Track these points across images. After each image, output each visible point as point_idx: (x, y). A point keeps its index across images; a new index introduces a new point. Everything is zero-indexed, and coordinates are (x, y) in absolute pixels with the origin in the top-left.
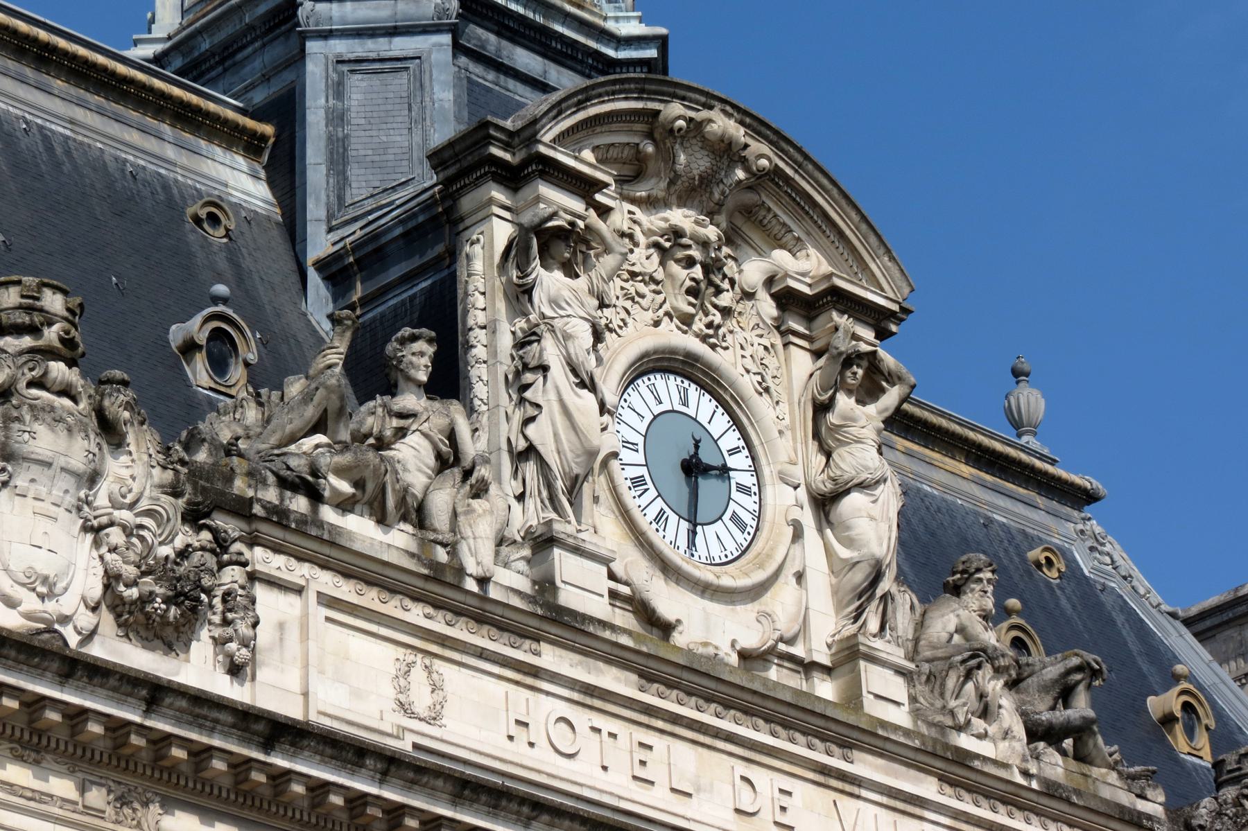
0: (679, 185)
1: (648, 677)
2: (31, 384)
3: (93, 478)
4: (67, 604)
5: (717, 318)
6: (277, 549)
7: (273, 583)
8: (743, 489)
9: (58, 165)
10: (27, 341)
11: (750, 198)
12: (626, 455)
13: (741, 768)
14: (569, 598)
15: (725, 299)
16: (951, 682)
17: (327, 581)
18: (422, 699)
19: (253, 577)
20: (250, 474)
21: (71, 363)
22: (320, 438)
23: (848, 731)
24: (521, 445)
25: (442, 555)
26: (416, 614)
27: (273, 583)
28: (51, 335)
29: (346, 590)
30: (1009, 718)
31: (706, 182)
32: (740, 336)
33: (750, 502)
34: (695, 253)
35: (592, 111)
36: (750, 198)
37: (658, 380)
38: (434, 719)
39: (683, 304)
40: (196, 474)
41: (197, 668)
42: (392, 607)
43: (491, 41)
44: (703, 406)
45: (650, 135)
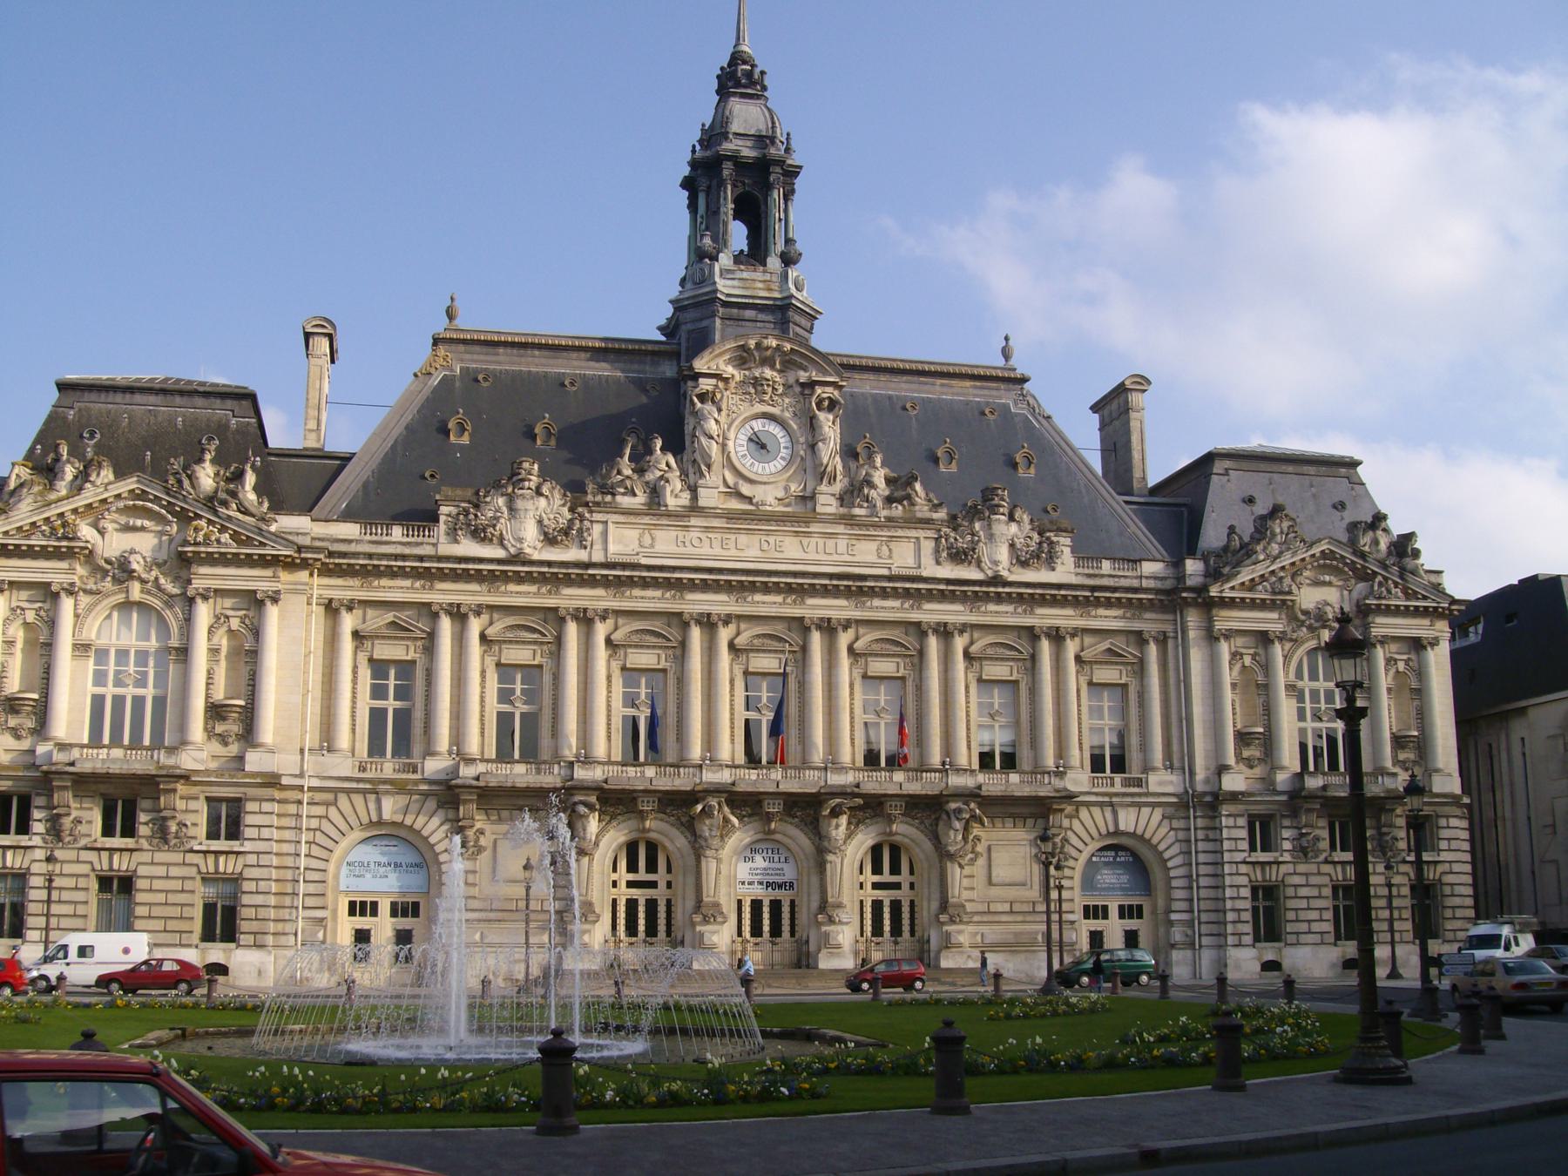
14: (701, 503)
23: (811, 516)
26: (647, 520)
29: (621, 518)
38: (652, 546)
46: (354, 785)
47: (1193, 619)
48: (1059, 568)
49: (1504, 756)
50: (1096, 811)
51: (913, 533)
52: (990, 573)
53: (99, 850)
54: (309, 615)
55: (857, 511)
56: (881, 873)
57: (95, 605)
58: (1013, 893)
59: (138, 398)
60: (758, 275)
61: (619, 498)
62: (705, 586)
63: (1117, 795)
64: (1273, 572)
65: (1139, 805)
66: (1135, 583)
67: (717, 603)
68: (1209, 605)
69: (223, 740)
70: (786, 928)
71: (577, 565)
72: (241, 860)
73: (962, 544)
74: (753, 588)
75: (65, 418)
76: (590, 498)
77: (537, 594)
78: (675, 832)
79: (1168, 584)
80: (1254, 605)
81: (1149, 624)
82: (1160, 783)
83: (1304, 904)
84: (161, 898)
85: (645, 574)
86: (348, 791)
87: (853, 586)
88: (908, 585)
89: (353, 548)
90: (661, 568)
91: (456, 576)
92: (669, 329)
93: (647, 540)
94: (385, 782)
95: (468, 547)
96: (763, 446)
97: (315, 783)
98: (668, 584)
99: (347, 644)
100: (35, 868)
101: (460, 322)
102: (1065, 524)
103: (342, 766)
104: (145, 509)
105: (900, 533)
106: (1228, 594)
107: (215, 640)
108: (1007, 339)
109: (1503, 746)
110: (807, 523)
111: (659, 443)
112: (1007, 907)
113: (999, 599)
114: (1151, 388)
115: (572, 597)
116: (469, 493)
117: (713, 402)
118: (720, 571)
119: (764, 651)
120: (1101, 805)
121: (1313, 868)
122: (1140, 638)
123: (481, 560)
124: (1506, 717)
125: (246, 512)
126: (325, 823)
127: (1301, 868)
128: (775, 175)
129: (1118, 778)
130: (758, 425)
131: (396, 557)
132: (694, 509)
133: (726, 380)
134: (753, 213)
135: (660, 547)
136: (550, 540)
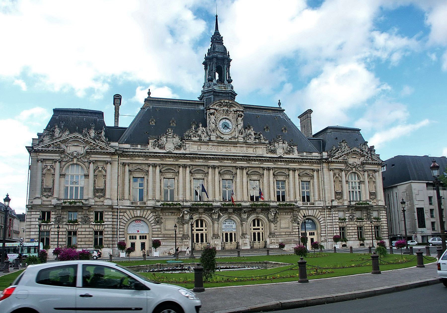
1: (218, 143)
17: (192, 143)
26: (199, 143)
29: (193, 143)
44: (227, 121)
47: (325, 165)
48: (295, 154)
49: (392, 196)
51: (261, 146)
52: (279, 156)
53: (68, 225)
54: (118, 166)
55: (248, 141)
56: (255, 226)
57: (65, 164)
58: (285, 230)
59: (74, 113)
60: (222, 85)
62: (213, 159)
63: (309, 207)
64: (343, 155)
65: (314, 209)
66: (312, 158)
67: (216, 163)
68: (329, 162)
69: (99, 197)
70: (233, 239)
71: (183, 154)
72: (104, 226)
73: (272, 148)
74: (224, 159)
75: (56, 118)
76: (185, 138)
79: (319, 158)
80: (339, 163)
81: (315, 167)
82: (318, 204)
83: (351, 231)
84: (84, 236)
86: (129, 209)
87: (247, 159)
89: (128, 150)
90: (203, 155)
91: (155, 157)
92: (201, 98)
93: (199, 148)
94: (138, 207)
95: (157, 150)
96: (226, 126)
97: (121, 207)
98: (205, 158)
99: (127, 173)
100: (52, 230)
101: (151, 96)
102: (295, 143)
103: (128, 203)
104: (78, 141)
106: (333, 160)
107: (96, 173)
109: (392, 195)
111: (201, 125)
112: (284, 234)
113: (281, 161)
115: (182, 162)
116: (156, 137)
117: (214, 115)
118: (217, 155)
120: (305, 209)
121: (353, 223)
122: (313, 170)
123: (160, 153)
124: (392, 188)
125: (103, 142)
127: (351, 223)
128: (226, 62)
129: (309, 203)
130: (224, 121)
131: (139, 152)
132: (210, 140)
133: (217, 110)
134: (220, 70)
135: (202, 150)
136: (176, 148)
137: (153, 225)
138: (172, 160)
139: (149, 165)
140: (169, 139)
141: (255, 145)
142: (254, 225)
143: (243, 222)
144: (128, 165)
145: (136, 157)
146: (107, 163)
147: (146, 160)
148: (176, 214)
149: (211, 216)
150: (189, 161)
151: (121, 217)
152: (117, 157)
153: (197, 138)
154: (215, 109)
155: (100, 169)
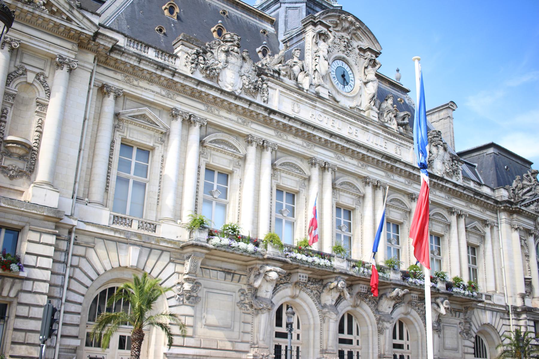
0: (343, 29)
1: (334, 109)
2: (231, 50)
3: (241, 67)
4: (237, 88)
5: (349, 52)
6: (272, 82)
7: (271, 88)
8: (352, 80)
9: (239, 21)
10: (231, 44)
11: (355, 32)
12: (332, 73)
13: (349, 126)
14: (321, 95)
15: (350, 49)
16: (385, 115)
18: (296, 109)
19: (268, 86)
20: (268, 69)
21: (238, 47)
22: (280, 65)
24: (315, 69)
25: (300, 86)
26: (296, 95)
27: (271, 88)
28: (235, 43)
29: (284, 90)
30: (395, 122)
31: (348, 28)
32: (352, 55)
33: (353, 83)
34: (346, 40)
35: (329, 14)
36: (355, 32)
37: (338, 61)
39: (343, 49)
40: (259, 68)
41: (258, 100)
42: (292, 94)
43: (312, 6)
44: (346, 66)
45: (339, 20)
46: (112, 234)
47: (503, 216)
50: (479, 310)
55: (386, 124)
61: (281, 77)
62: (326, 144)
71: (266, 109)
77: (237, 122)
78: (309, 300)
85: (299, 127)
88: (411, 171)
91: (193, 95)
94: (136, 234)
96: (343, 76)
99: (108, 121)
105: (403, 142)
108: (398, 71)
110: (367, 124)
111: (297, 54)
114: (456, 109)
119: (347, 192)
126: (83, 260)
130: (340, 63)
137: (173, 302)
138: (233, 117)
139: (174, 114)
140: (232, 59)
141: (399, 138)
142: (394, 337)
143: (386, 325)
144: (116, 97)
145: (144, 78)
146: (60, 63)
147: (168, 96)
148: (237, 277)
149: (318, 298)
150: (272, 132)
151: (75, 261)
152: (90, 57)
153: (291, 81)
154: (328, 27)
155: (31, 77)
